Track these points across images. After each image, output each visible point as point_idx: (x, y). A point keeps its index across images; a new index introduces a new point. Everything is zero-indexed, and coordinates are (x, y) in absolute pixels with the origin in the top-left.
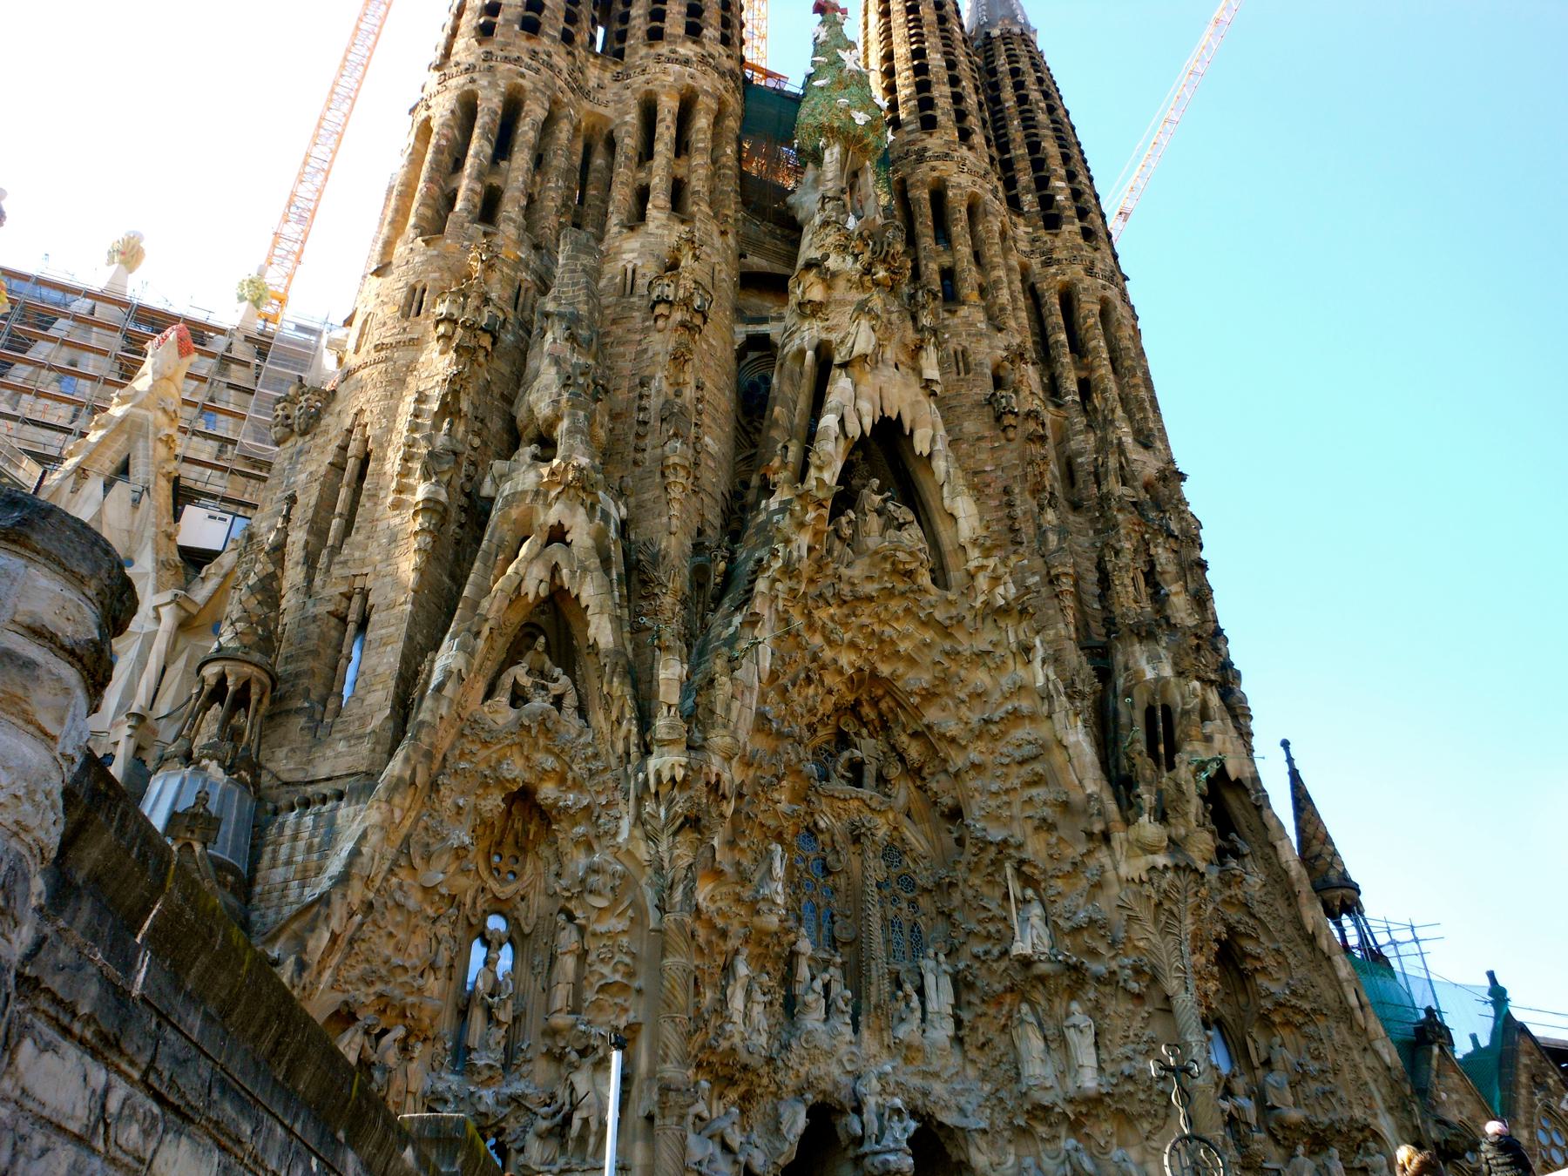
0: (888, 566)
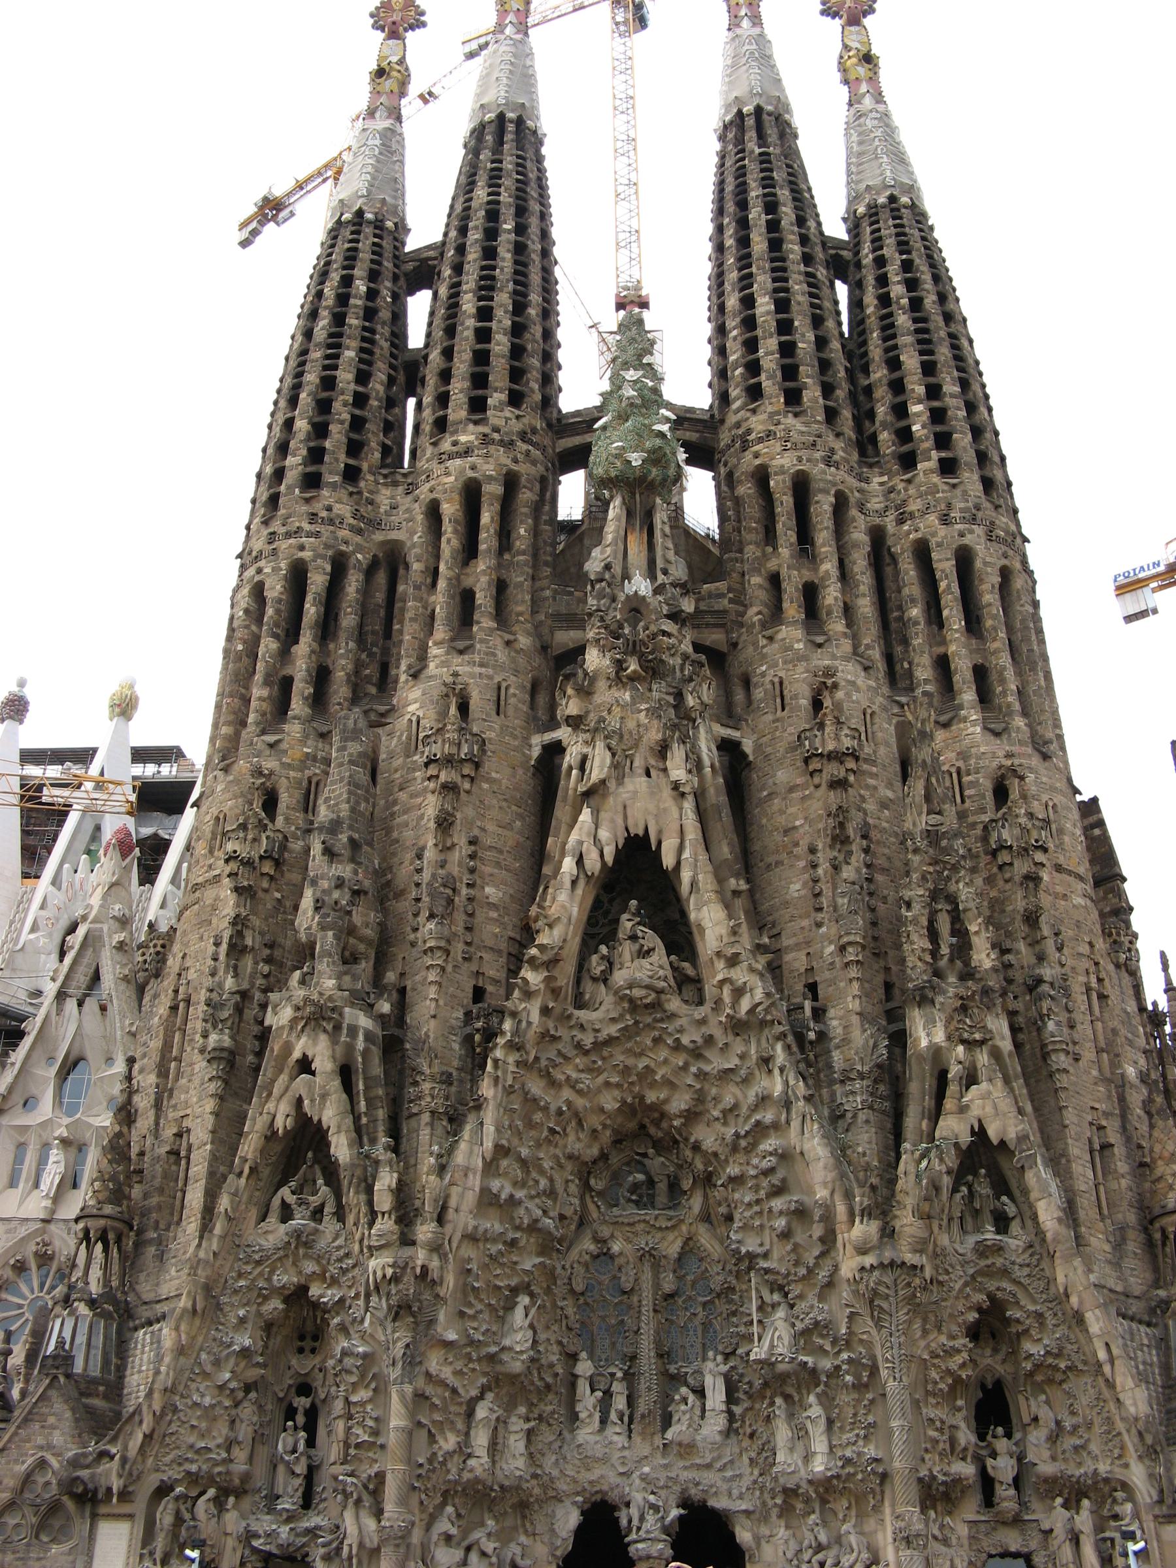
0: (626, 1005)
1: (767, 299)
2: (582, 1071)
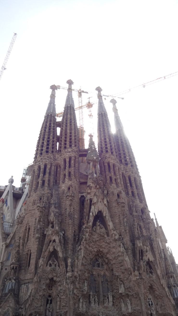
0: (100, 236)
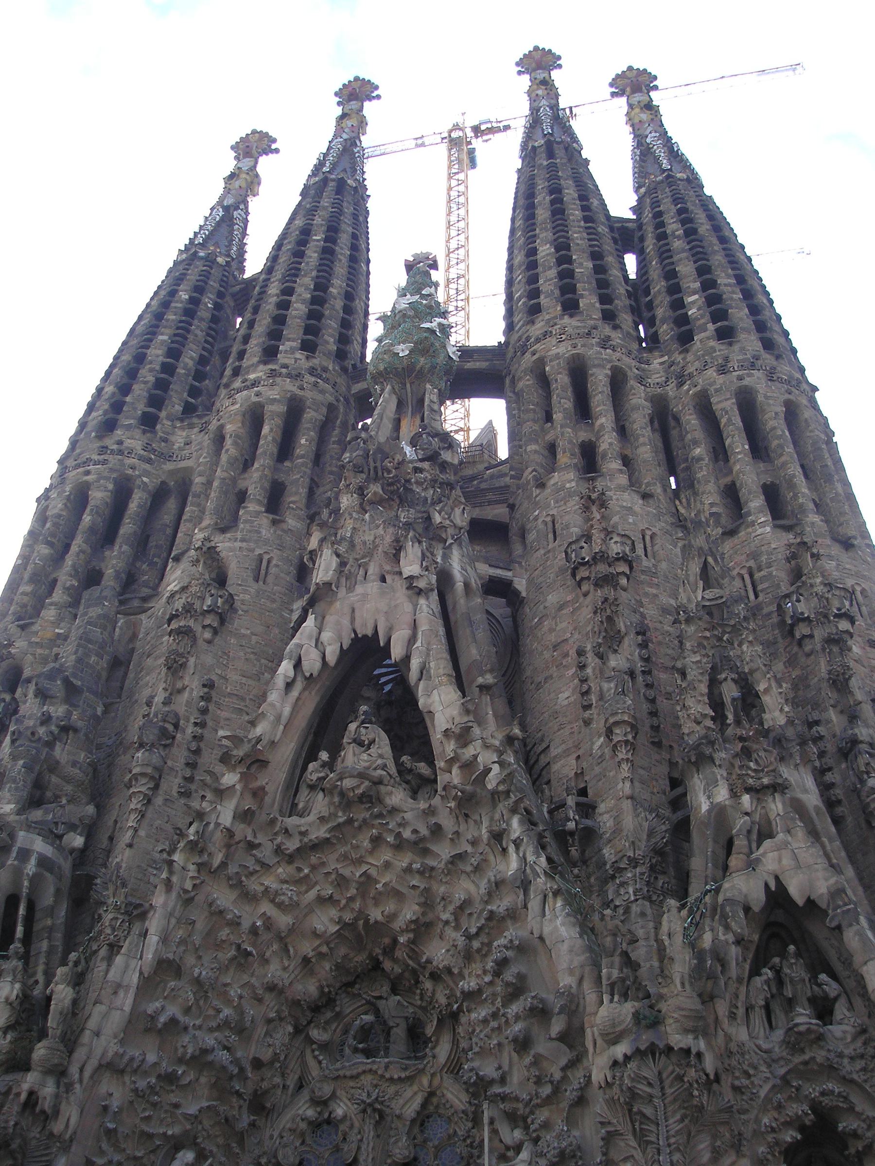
0: (336, 799)
1: (548, 246)
2: (286, 882)
